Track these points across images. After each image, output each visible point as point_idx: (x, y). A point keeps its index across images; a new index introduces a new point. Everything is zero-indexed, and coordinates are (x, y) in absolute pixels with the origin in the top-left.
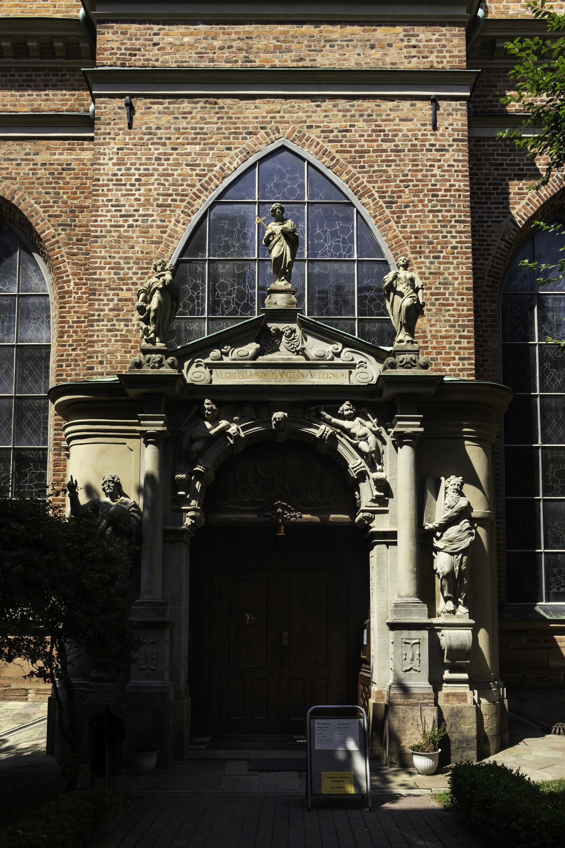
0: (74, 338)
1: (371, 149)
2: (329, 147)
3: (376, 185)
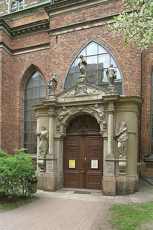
2: (104, 39)
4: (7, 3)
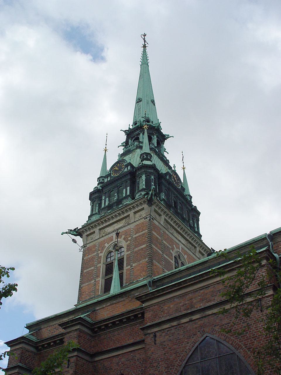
1: (239, 328)
3: (243, 342)
4: (100, 255)
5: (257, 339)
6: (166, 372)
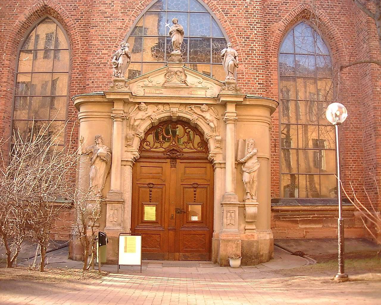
0: (80, 70)
3: (220, 6)
5: (236, 7)
6: (121, 13)
